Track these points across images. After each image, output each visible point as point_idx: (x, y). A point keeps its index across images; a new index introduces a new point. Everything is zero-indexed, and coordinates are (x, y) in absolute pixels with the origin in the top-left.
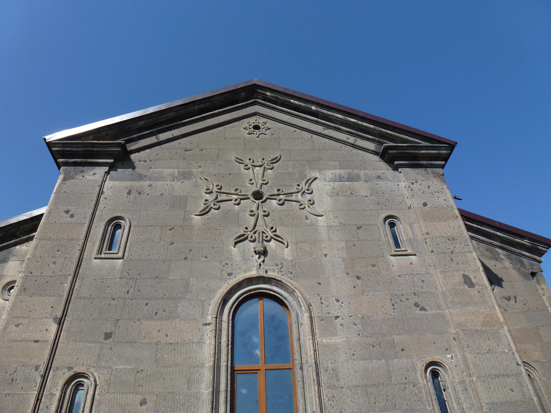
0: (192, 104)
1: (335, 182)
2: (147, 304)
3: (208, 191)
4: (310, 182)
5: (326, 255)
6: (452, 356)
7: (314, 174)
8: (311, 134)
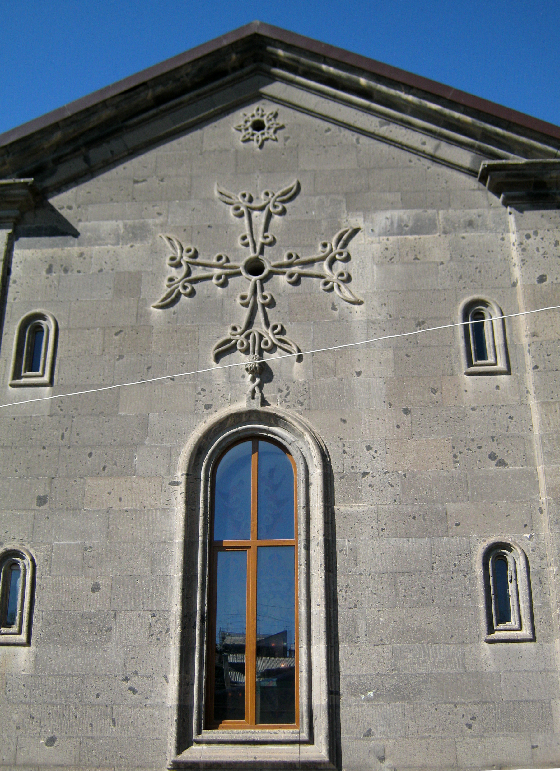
0: (141, 88)
1: (391, 234)
2: (90, 455)
3: (175, 262)
4: (344, 237)
5: (359, 374)
6: (531, 536)
7: (356, 221)
8: (357, 135)
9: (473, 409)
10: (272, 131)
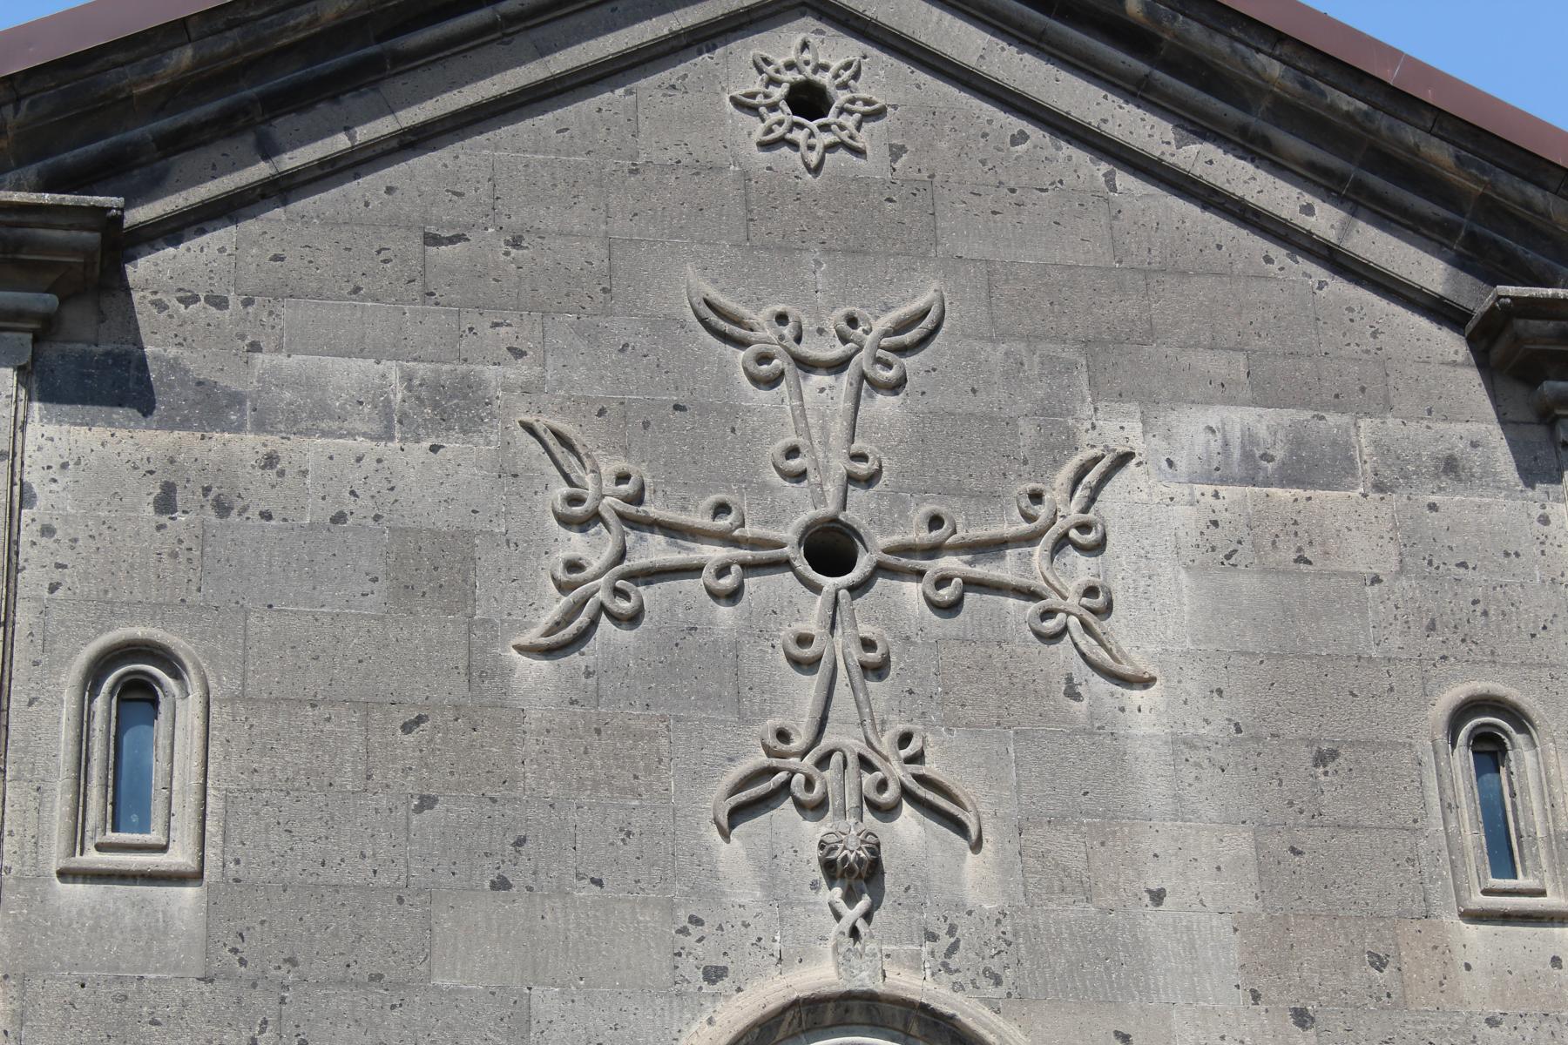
1: (1223, 481)
3: (578, 510)
5: (1158, 897)
9: (1492, 1022)
10: (849, 121)
